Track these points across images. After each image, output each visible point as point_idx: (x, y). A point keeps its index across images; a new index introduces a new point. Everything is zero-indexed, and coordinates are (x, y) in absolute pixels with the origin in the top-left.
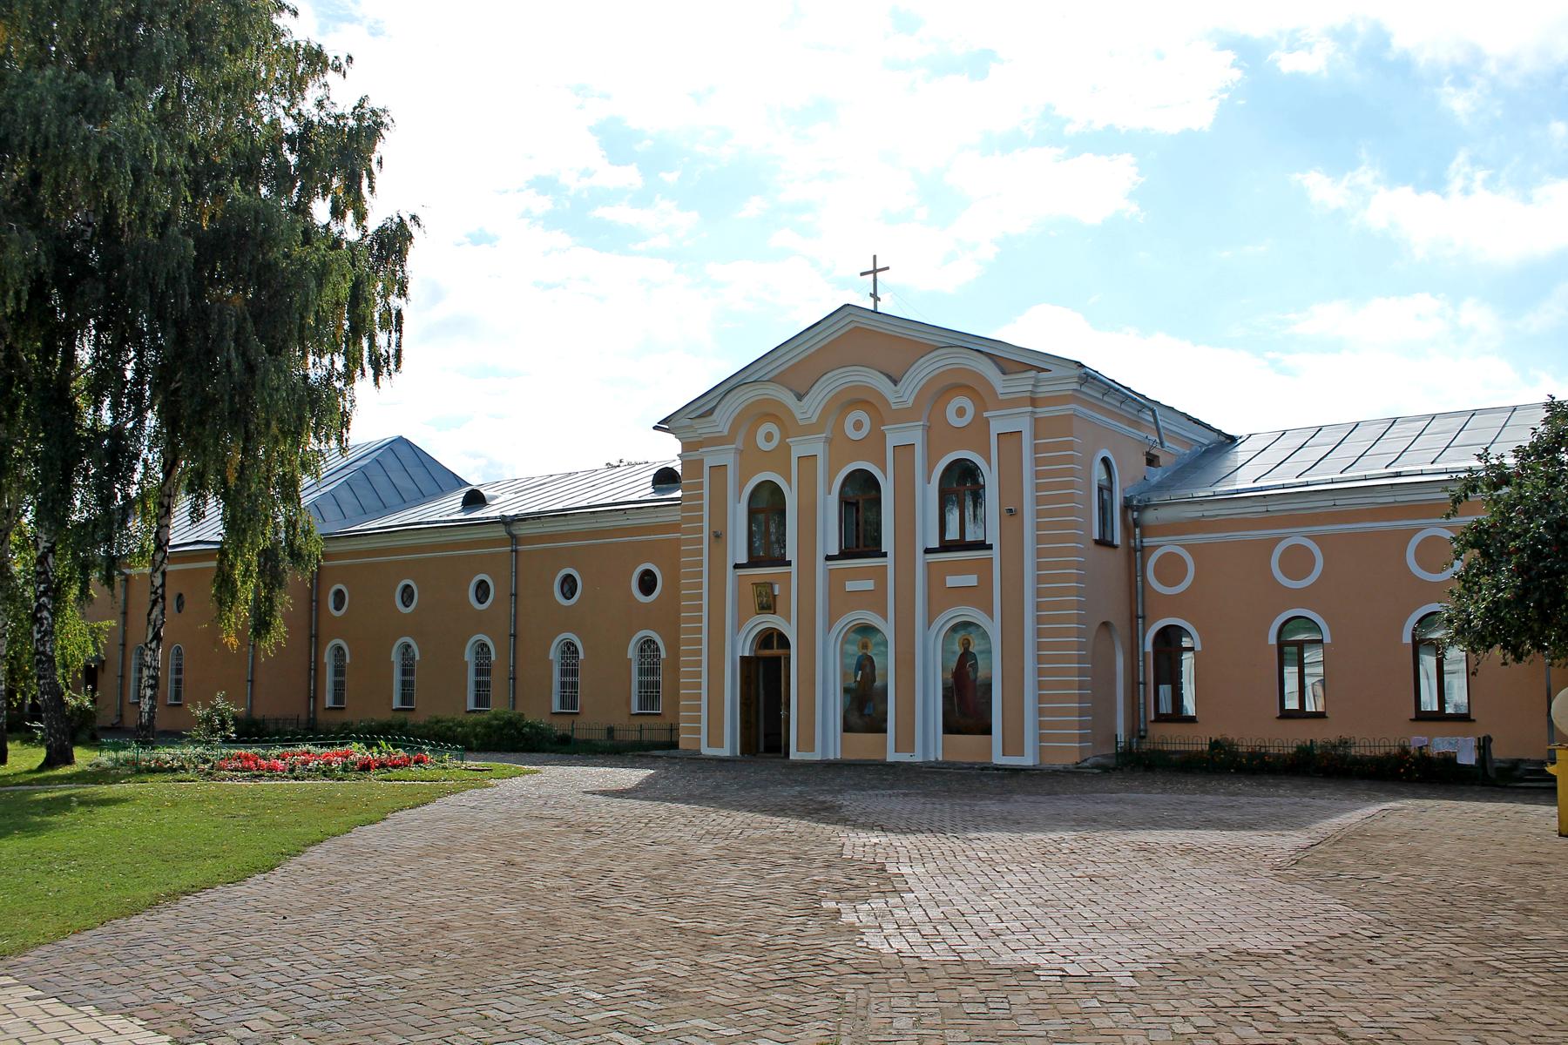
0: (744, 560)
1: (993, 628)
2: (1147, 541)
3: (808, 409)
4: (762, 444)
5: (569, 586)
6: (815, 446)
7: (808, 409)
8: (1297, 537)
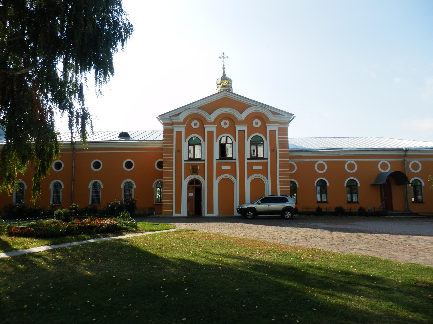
0: (187, 159)
3: (212, 117)
7: (212, 117)
8: (321, 161)
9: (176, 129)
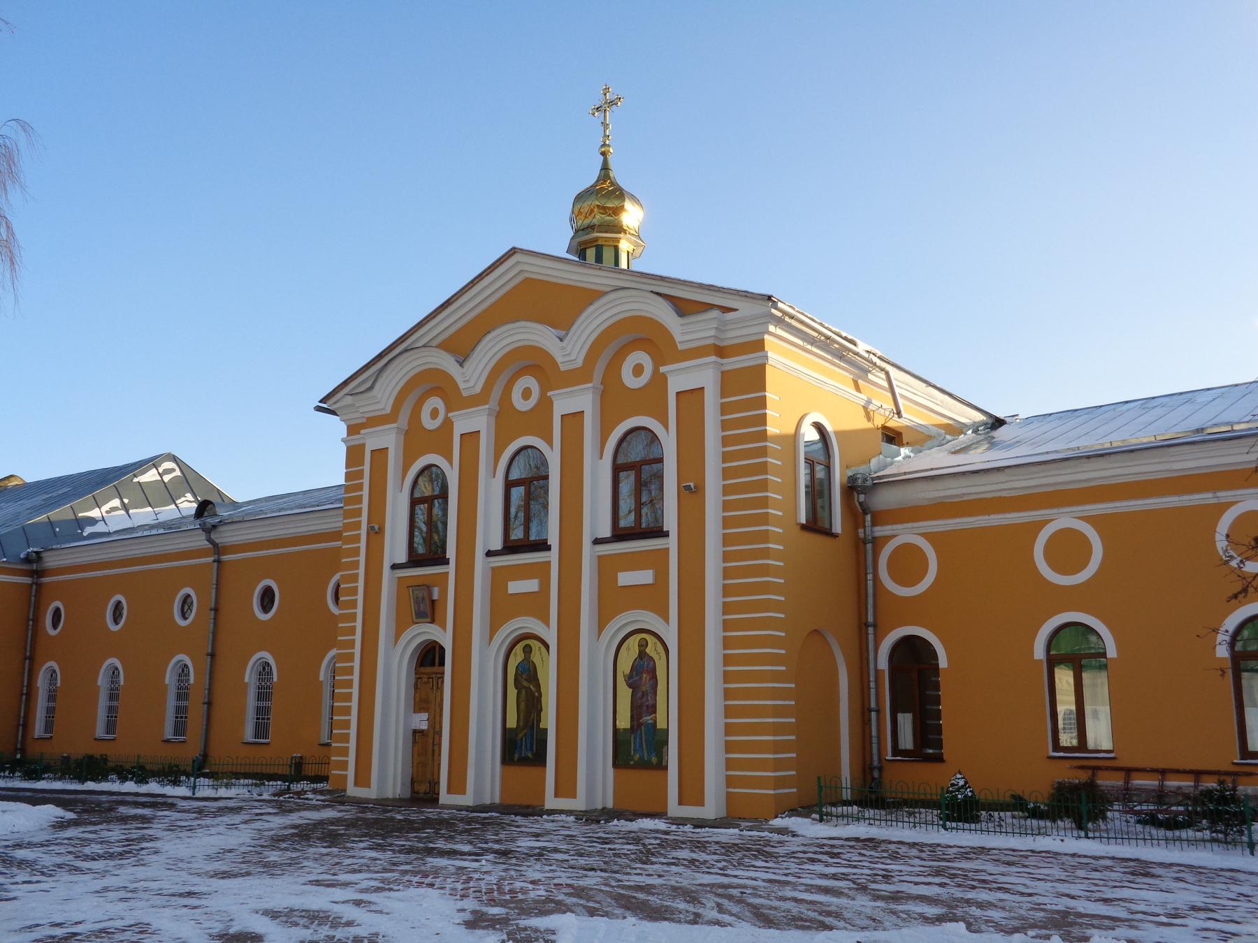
1: (671, 634)
2: (880, 531)
3: (470, 377)
4: (429, 423)
5: (267, 598)
6: (476, 421)
8: (1064, 519)
9: (374, 440)
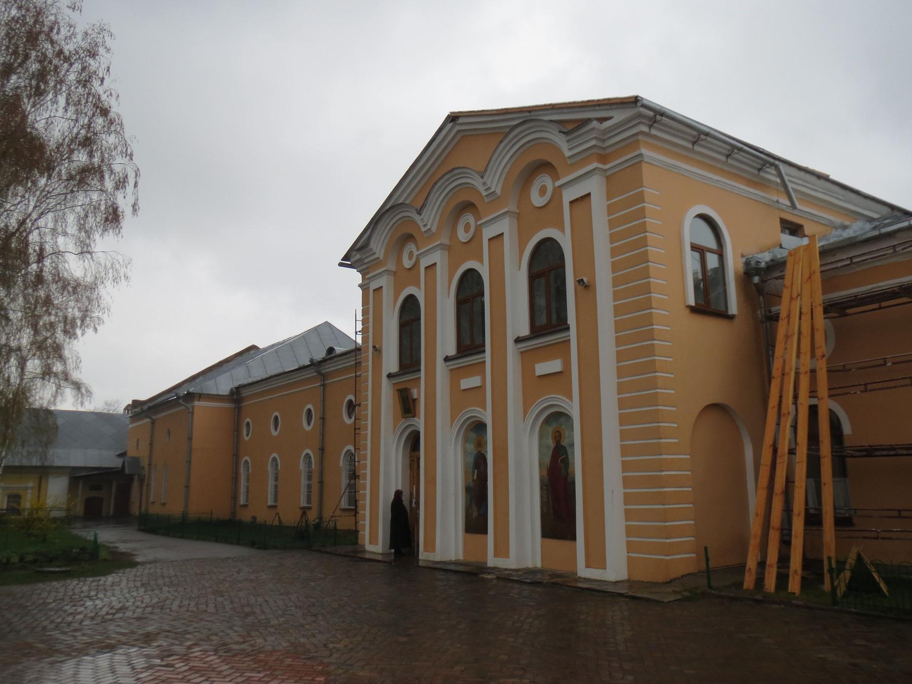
7: (429, 219)
